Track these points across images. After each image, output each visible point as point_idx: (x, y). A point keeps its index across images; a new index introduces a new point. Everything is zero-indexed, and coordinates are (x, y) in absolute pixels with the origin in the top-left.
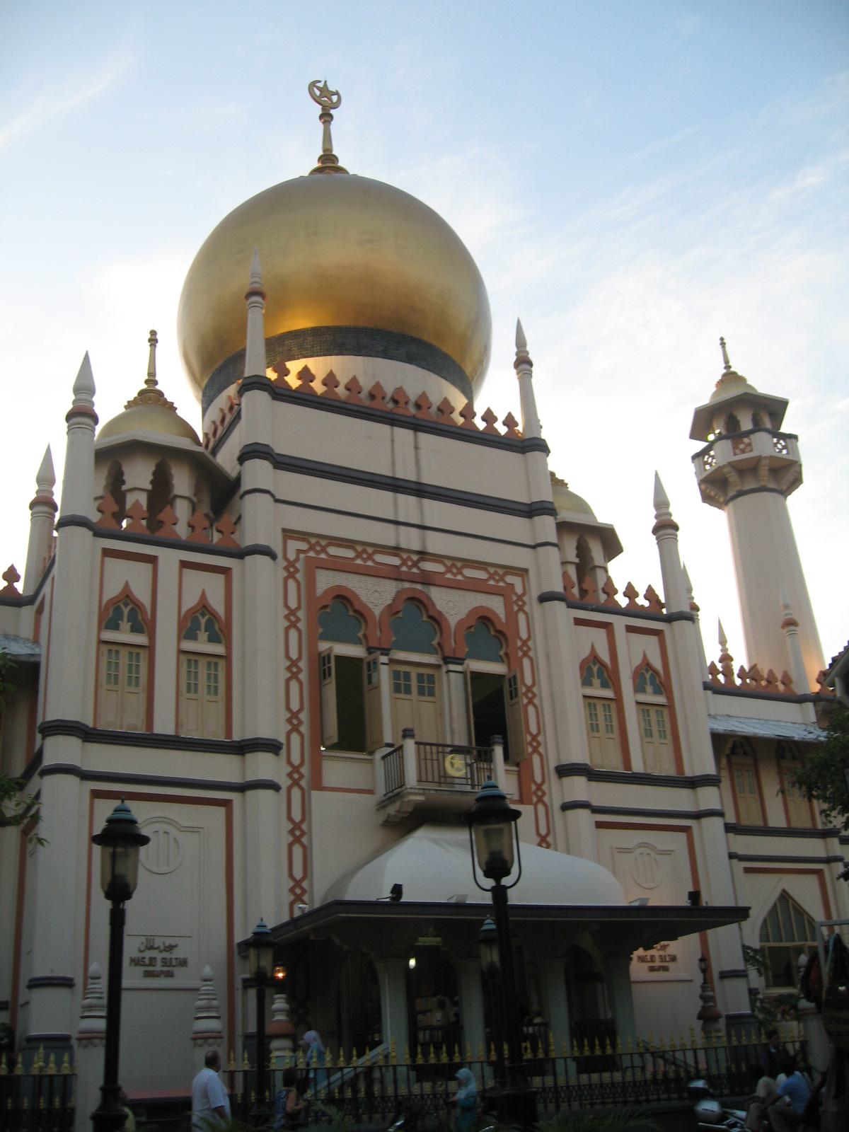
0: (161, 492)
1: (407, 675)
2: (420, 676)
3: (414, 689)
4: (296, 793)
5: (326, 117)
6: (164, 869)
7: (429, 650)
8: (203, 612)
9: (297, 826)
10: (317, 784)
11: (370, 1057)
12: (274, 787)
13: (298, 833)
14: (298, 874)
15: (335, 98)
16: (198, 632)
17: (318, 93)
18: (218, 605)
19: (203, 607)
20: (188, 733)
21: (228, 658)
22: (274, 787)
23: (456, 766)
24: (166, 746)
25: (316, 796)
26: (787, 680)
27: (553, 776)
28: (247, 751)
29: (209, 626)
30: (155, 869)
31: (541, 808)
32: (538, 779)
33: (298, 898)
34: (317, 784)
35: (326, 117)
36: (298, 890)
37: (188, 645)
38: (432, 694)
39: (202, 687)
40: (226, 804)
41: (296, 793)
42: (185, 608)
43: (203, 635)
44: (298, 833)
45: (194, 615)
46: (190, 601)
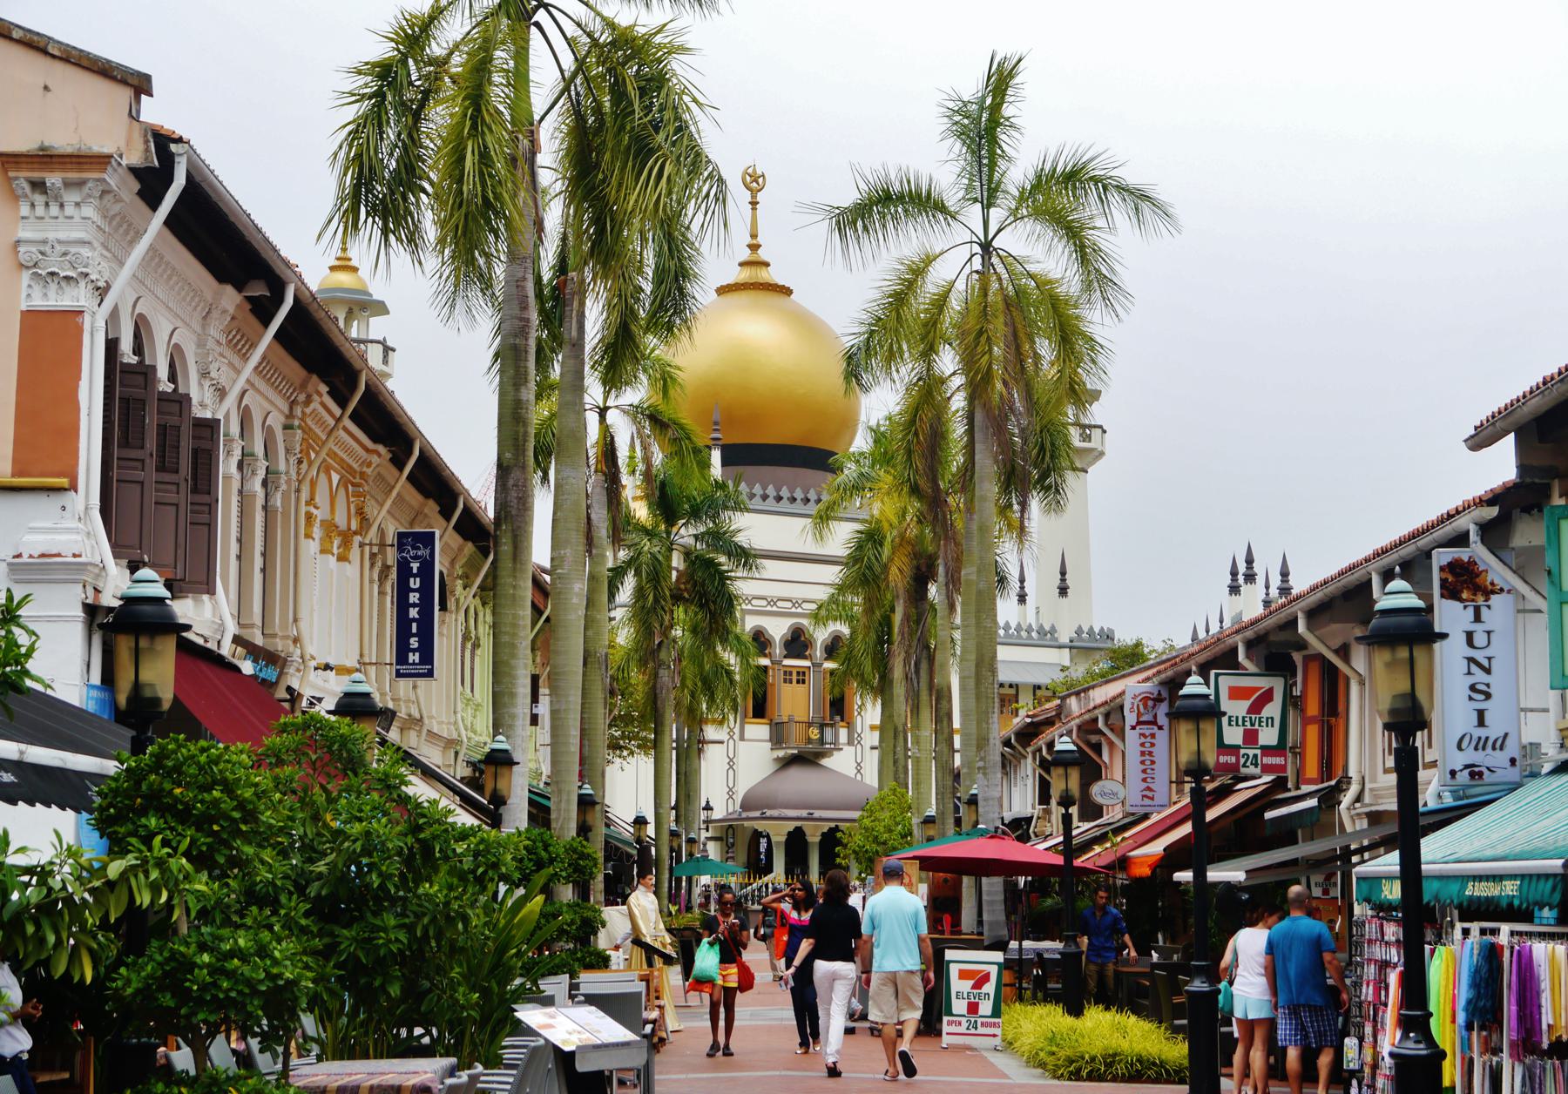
1: (791, 673)
2: (798, 673)
3: (794, 681)
4: (731, 742)
5: (754, 204)
7: (805, 658)
9: (731, 760)
10: (742, 738)
11: (765, 879)
12: (722, 742)
13: (731, 763)
14: (731, 785)
15: (761, 180)
17: (748, 178)
22: (722, 742)
23: (814, 733)
25: (741, 745)
26: (1053, 630)
27: (867, 728)
31: (859, 747)
32: (859, 731)
33: (731, 797)
34: (742, 738)
35: (754, 204)
36: (731, 793)
38: (804, 682)
41: (731, 742)
44: (731, 763)
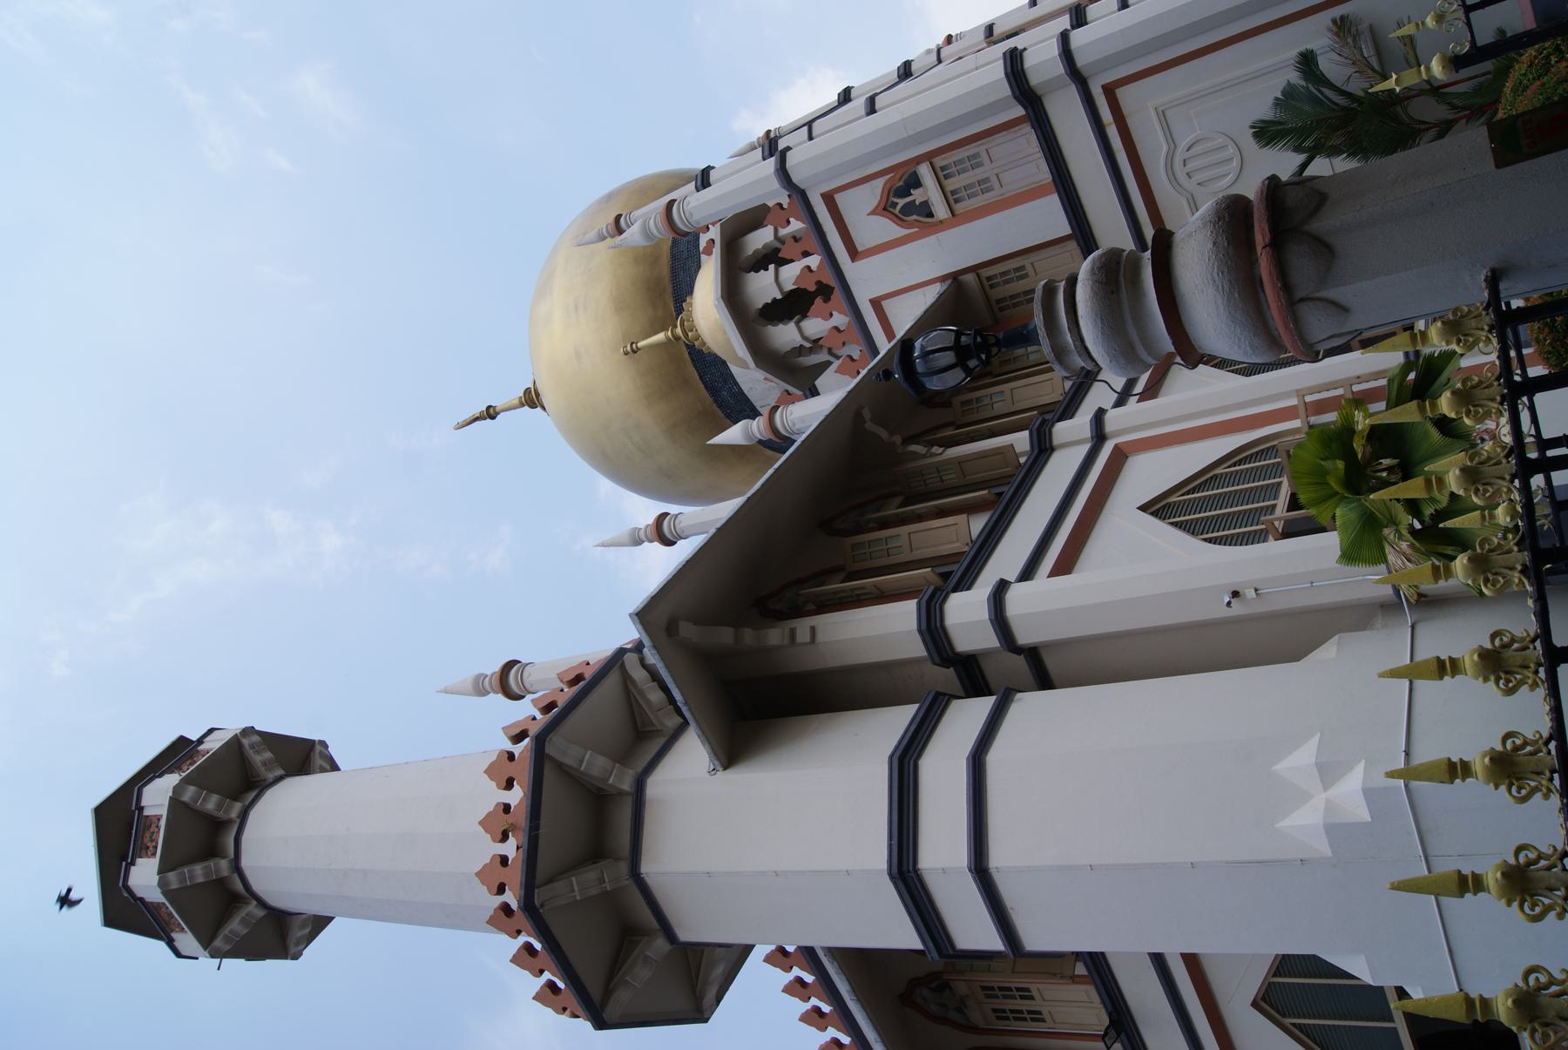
0: (793, 305)
6: (1231, 150)
8: (891, 207)
16: (917, 203)
18: (872, 194)
19: (885, 209)
20: (1044, 174)
21: (929, 157)
24: (1072, 187)
28: (1027, 87)
29: (904, 192)
30: (1235, 163)
37: (941, 211)
39: (979, 174)
40: (1110, 91)
42: (898, 232)
43: (917, 196)
45: (900, 216)
46: (887, 229)
